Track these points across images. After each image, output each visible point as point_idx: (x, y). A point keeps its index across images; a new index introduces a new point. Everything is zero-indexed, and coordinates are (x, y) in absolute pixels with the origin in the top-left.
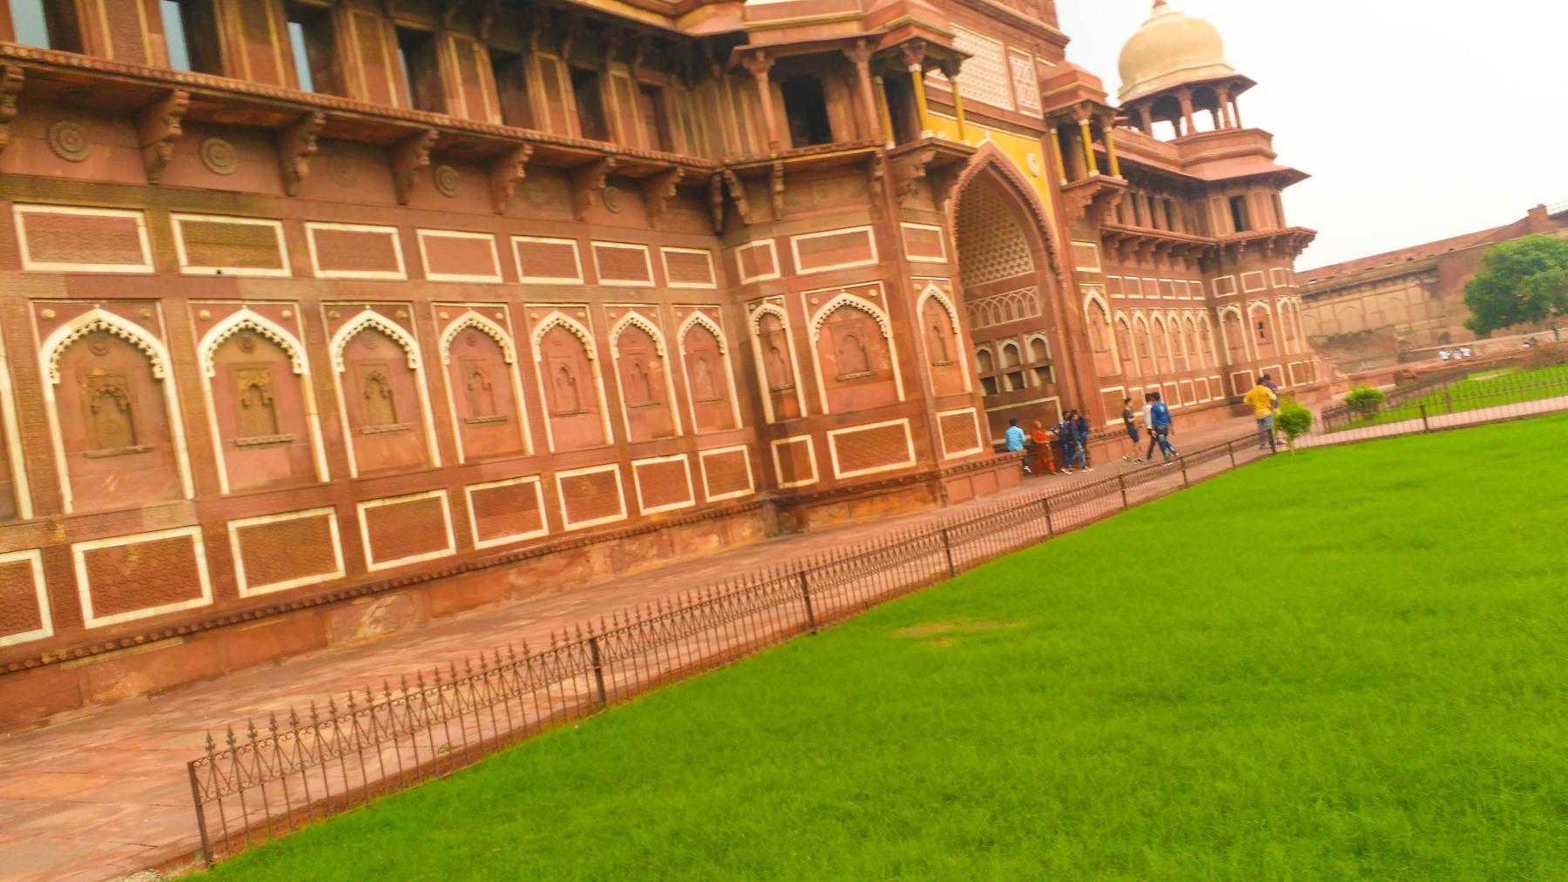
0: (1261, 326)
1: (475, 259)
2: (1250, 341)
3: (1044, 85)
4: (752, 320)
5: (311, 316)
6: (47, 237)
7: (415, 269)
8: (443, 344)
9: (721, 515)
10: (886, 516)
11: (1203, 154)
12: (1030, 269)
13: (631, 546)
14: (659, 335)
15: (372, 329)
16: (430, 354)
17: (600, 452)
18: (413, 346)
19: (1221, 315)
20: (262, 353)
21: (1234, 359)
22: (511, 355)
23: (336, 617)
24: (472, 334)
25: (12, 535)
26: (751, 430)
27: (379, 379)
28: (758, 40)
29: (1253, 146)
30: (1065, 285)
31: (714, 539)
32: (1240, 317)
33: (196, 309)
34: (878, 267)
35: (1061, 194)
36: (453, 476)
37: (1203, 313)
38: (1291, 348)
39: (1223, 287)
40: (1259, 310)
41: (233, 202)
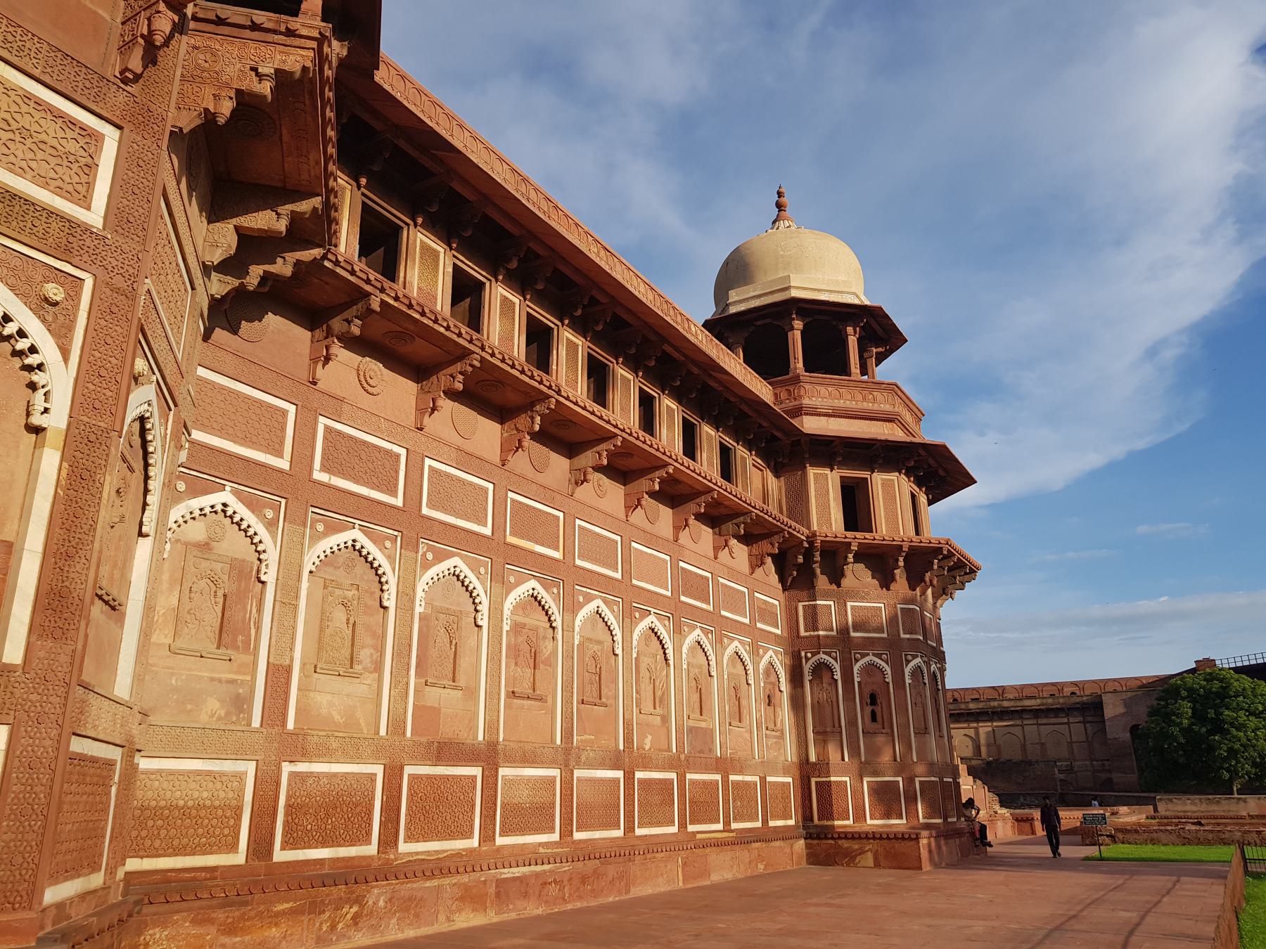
0: (873, 699)
2: (852, 723)
19: (807, 668)
32: (838, 676)
37: (774, 656)
40: (871, 669)
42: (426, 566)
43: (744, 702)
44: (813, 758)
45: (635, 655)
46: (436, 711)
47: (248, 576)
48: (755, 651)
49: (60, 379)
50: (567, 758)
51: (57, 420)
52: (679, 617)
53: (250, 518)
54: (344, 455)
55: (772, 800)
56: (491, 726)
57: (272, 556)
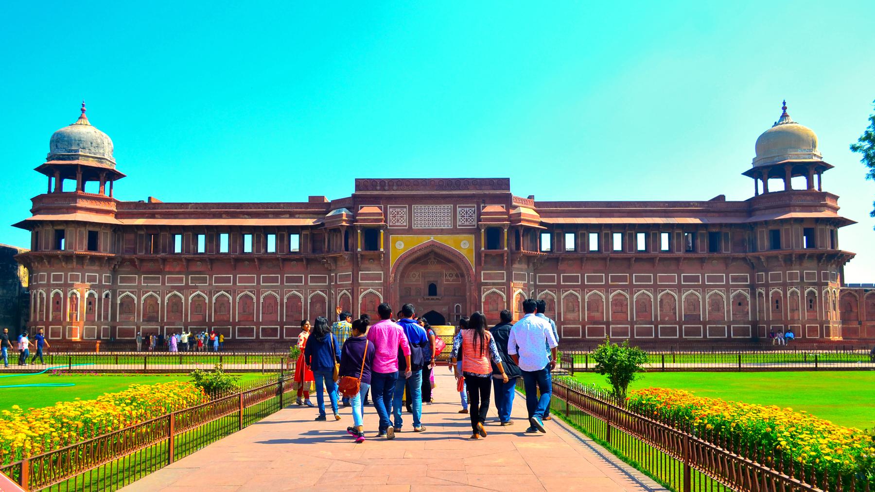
0: (777, 302)
1: (251, 280)
2: (768, 309)
3: (480, 214)
5: (210, 292)
6: (171, 280)
7: (235, 283)
8: (238, 298)
14: (302, 297)
15: (222, 295)
17: (276, 323)
18: (231, 298)
22: (255, 300)
24: (247, 296)
27: (222, 303)
30: (473, 287)
36: (234, 324)
38: (792, 317)
39: (760, 278)
46: (594, 317)
48: (728, 291)
49: (505, 297)
50: (632, 323)
51: (505, 300)
52: (679, 288)
54: (566, 279)
55: (745, 331)
56: (608, 318)
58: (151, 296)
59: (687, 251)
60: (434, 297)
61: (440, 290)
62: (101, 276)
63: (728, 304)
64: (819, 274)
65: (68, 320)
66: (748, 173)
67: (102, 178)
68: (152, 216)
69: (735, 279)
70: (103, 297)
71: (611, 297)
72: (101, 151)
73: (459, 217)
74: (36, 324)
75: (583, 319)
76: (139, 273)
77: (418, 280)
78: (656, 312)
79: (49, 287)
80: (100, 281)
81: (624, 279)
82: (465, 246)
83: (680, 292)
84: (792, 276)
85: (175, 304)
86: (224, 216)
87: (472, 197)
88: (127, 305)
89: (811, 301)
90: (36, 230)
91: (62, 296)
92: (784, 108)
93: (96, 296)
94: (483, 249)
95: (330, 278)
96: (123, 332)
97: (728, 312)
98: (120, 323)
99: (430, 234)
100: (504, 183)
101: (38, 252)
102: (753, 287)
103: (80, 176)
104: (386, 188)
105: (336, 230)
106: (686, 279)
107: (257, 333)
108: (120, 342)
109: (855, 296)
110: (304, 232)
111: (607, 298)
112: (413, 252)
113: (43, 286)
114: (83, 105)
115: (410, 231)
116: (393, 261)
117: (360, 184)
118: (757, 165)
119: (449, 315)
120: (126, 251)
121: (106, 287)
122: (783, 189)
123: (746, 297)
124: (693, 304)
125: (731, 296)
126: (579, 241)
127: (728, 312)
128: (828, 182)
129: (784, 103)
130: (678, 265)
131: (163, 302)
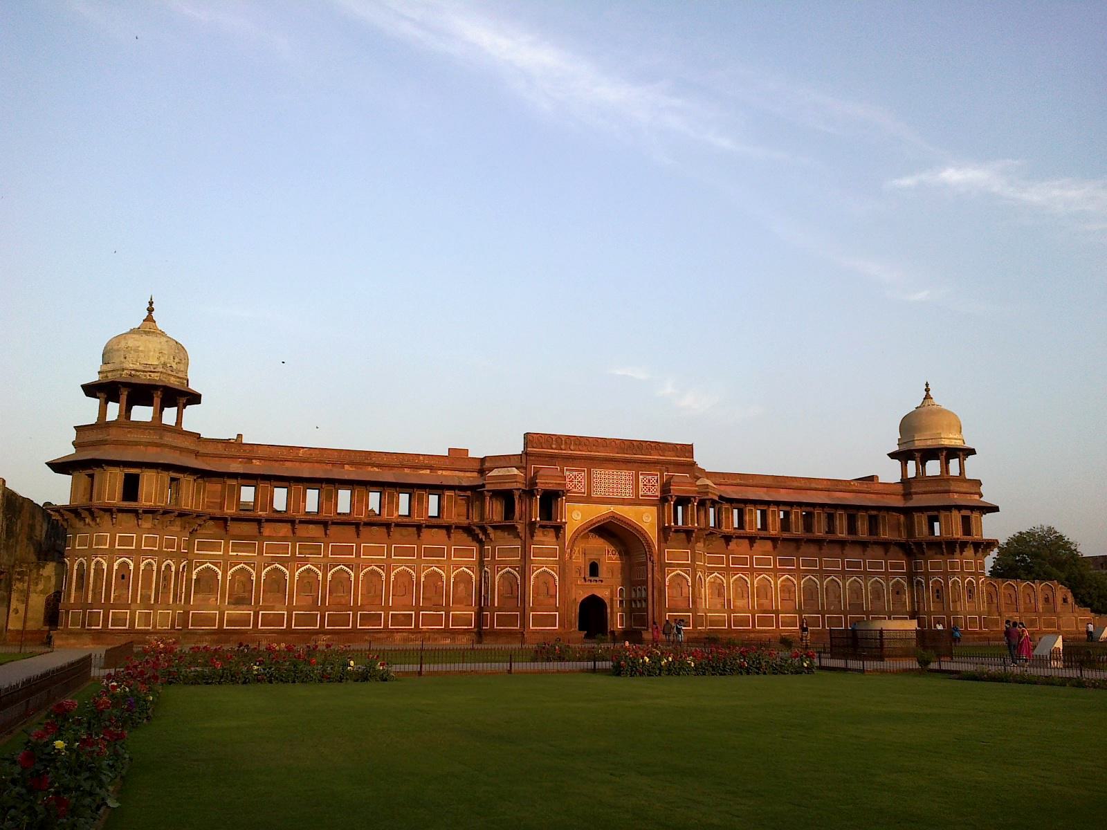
4: (483, 571)
5: (325, 567)
6: (270, 549)
7: (358, 555)
9: (454, 632)
10: (508, 643)
11: (913, 490)
12: (644, 560)
13: (411, 636)
15: (341, 569)
16: (357, 577)
18: (353, 575)
19: (915, 581)
20: (312, 574)
21: (919, 608)
22: (384, 578)
23: (314, 637)
24: (373, 572)
25: (248, 607)
26: (477, 607)
27: (340, 582)
28: (488, 487)
29: (947, 488)
30: (656, 568)
31: (448, 641)
33: (298, 564)
34: (520, 560)
35: (664, 531)
36: (356, 608)
41: (313, 539)
42: (756, 577)
43: (882, 595)
44: (916, 609)
45: (825, 587)
47: (721, 585)
49: (690, 580)
51: (690, 584)
52: (844, 574)
53: (720, 576)
56: (777, 606)
57: (725, 582)
58: (242, 569)
59: (827, 532)
60: (597, 579)
61: (603, 570)
62: (180, 539)
63: (888, 593)
64: (976, 563)
65: (139, 602)
66: (893, 456)
67: (181, 405)
68: (250, 459)
69: (893, 566)
70: (181, 570)
71: (779, 582)
72: (182, 367)
73: (641, 485)
74: (85, 606)
75: (753, 607)
76: (227, 535)
77: (579, 561)
78: (822, 599)
79: (112, 554)
80: (179, 547)
81: (791, 563)
82: (646, 519)
83: (844, 578)
84: (953, 566)
85: (276, 583)
86: (347, 467)
87: (656, 463)
88: (206, 583)
89: (970, 591)
90: (90, 472)
91: (132, 567)
92: (927, 390)
93: (173, 569)
94: (673, 524)
95: (482, 554)
96: (199, 620)
97: (889, 601)
98: (197, 607)
99: (610, 504)
100: (688, 449)
101: (96, 502)
102: (910, 576)
103: (157, 401)
104: (563, 447)
105: (496, 494)
106: (850, 564)
107: (386, 620)
108: (193, 633)
109: (996, 588)
110: (448, 493)
111: (776, 583)
112: (591, 523)
113: (103, 552)
114: (151, 303)
115: (588, 499)
116: (569, 532)
117: (529, 438)
118: (905, 448)
119: (612, 600)
120: (209, 507)
121: (185, 556)
122: (939, 474)
123: (903, 585)
124: (857, 592)
125: (891, 584)
126: (747, 518)
127: (889, 601)
128: (973, 468)
129: (927, 385)
130: (843, 549)
131: (259, 577)
